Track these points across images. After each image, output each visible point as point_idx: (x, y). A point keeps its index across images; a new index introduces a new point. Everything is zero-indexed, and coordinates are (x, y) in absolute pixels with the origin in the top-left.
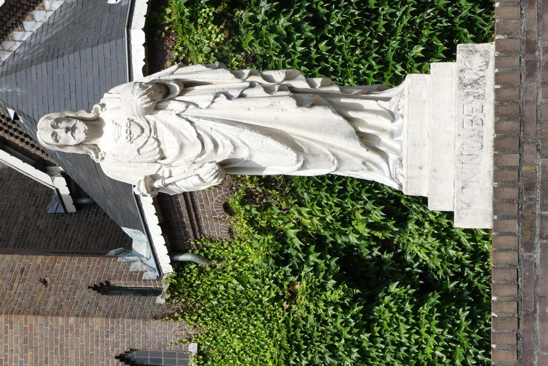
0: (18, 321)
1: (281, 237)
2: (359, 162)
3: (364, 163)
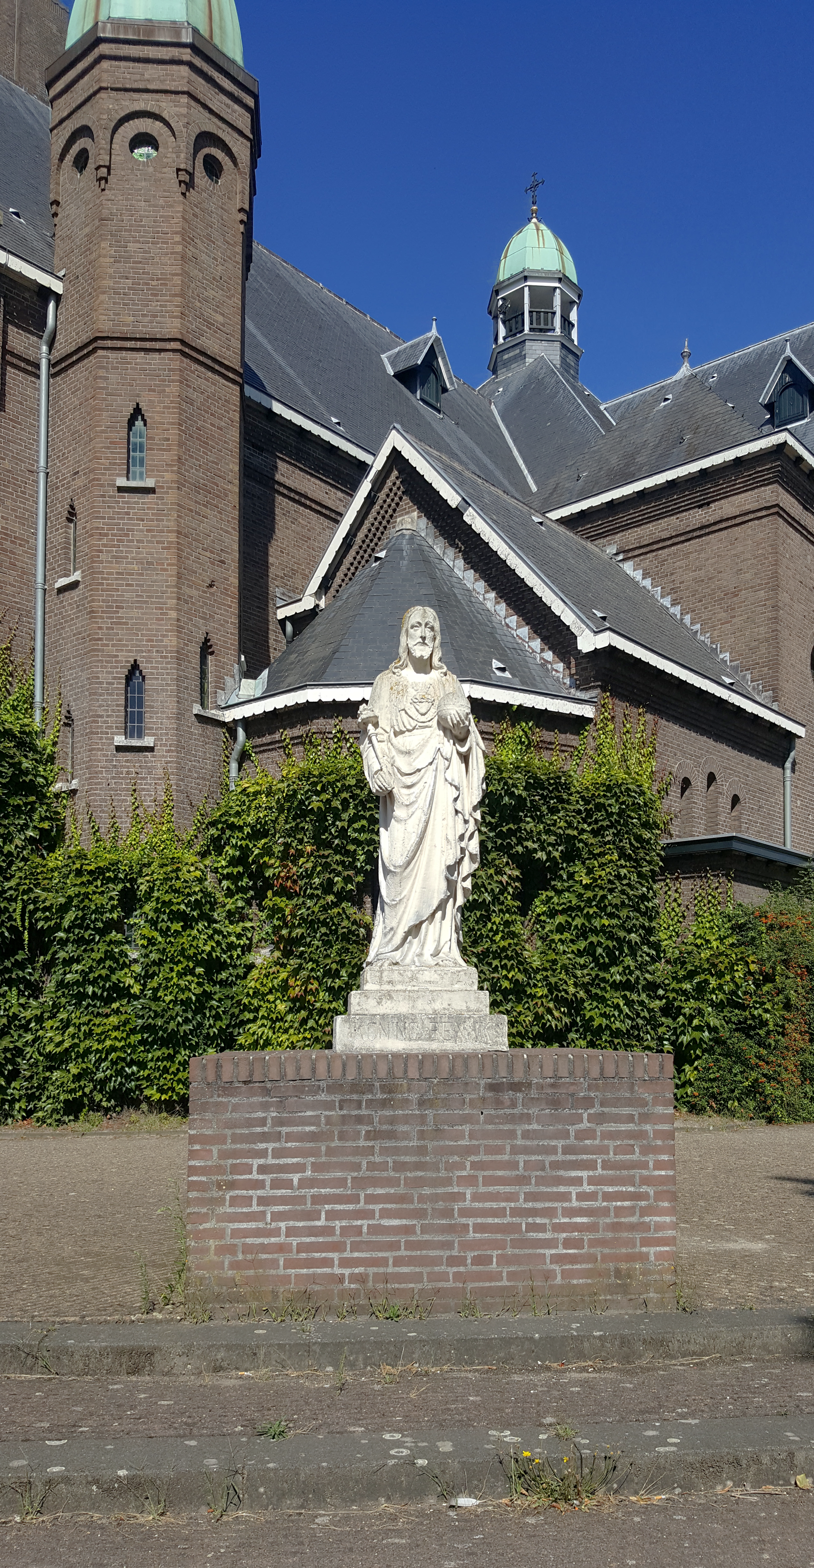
0: (170, 556)
2: (394, 924)
3: (392, 929)
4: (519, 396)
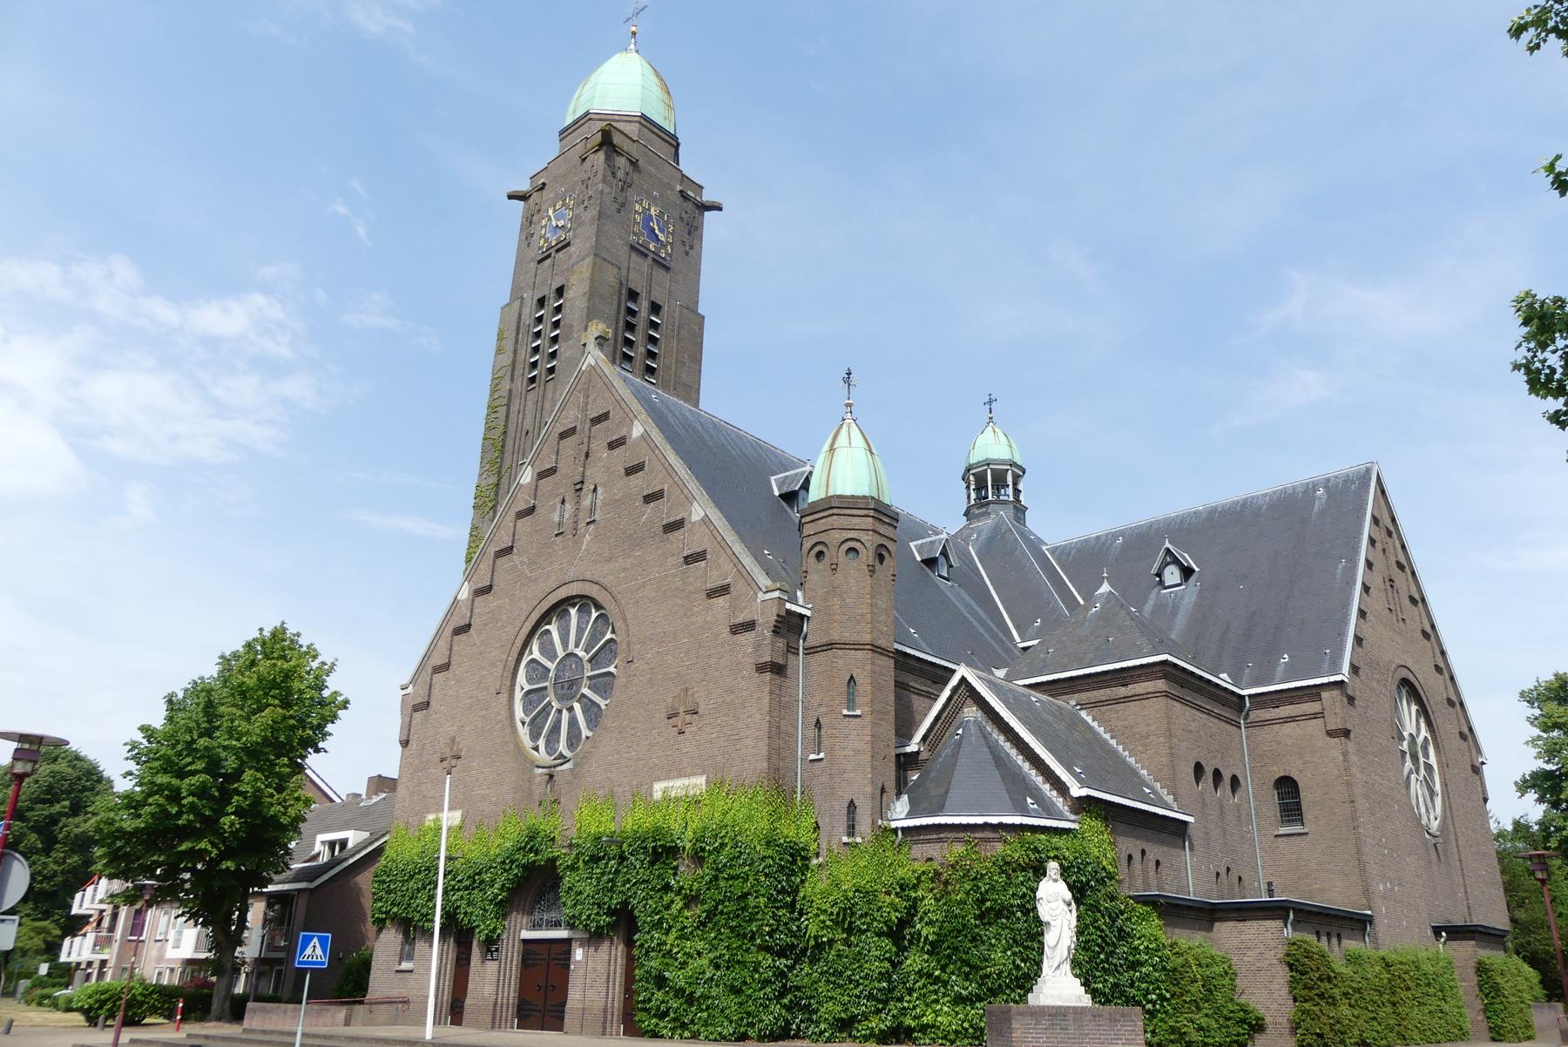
0: (868, 747)
1: (915, 887)
4: (991, 540)
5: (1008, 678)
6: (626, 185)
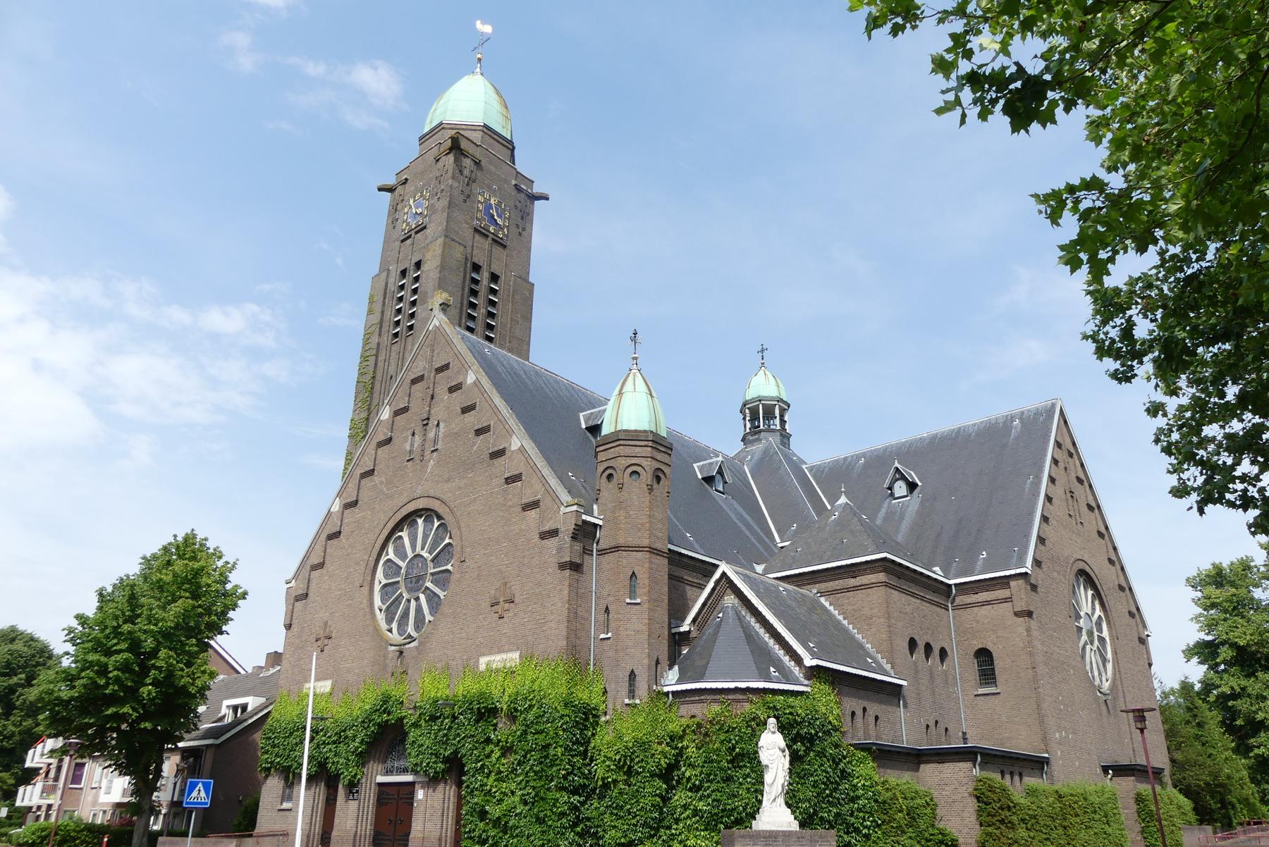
0: (645, 628)
1: (681, 738)
5: (766, 572)
6: (471, 181)
